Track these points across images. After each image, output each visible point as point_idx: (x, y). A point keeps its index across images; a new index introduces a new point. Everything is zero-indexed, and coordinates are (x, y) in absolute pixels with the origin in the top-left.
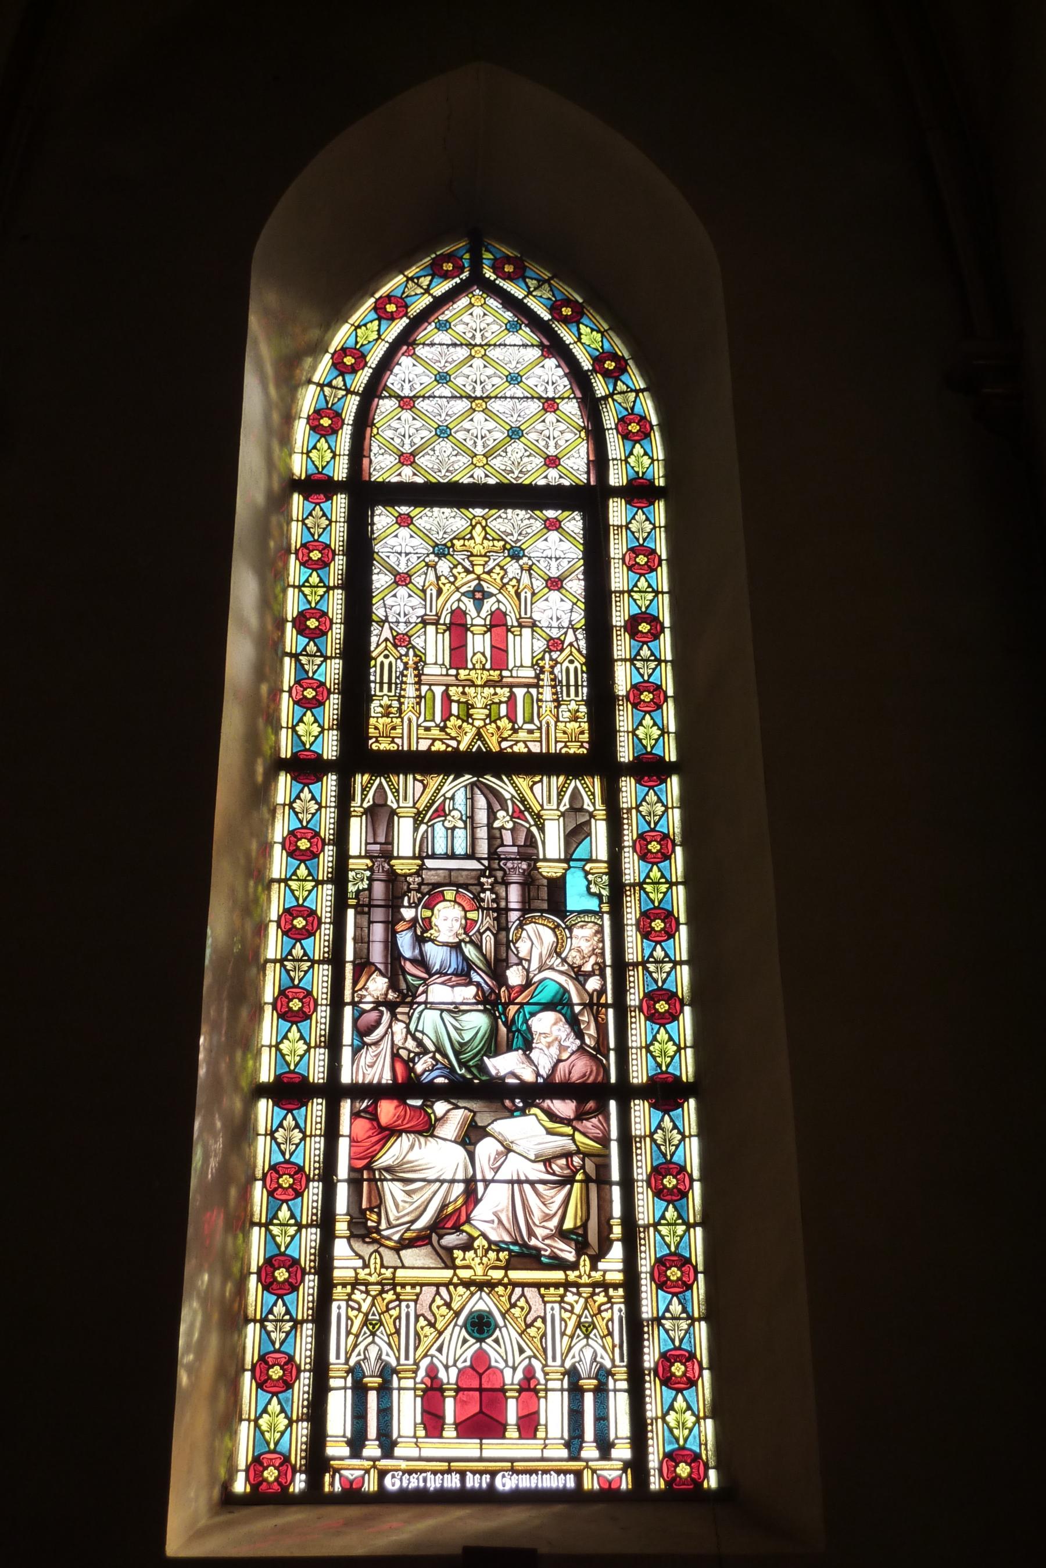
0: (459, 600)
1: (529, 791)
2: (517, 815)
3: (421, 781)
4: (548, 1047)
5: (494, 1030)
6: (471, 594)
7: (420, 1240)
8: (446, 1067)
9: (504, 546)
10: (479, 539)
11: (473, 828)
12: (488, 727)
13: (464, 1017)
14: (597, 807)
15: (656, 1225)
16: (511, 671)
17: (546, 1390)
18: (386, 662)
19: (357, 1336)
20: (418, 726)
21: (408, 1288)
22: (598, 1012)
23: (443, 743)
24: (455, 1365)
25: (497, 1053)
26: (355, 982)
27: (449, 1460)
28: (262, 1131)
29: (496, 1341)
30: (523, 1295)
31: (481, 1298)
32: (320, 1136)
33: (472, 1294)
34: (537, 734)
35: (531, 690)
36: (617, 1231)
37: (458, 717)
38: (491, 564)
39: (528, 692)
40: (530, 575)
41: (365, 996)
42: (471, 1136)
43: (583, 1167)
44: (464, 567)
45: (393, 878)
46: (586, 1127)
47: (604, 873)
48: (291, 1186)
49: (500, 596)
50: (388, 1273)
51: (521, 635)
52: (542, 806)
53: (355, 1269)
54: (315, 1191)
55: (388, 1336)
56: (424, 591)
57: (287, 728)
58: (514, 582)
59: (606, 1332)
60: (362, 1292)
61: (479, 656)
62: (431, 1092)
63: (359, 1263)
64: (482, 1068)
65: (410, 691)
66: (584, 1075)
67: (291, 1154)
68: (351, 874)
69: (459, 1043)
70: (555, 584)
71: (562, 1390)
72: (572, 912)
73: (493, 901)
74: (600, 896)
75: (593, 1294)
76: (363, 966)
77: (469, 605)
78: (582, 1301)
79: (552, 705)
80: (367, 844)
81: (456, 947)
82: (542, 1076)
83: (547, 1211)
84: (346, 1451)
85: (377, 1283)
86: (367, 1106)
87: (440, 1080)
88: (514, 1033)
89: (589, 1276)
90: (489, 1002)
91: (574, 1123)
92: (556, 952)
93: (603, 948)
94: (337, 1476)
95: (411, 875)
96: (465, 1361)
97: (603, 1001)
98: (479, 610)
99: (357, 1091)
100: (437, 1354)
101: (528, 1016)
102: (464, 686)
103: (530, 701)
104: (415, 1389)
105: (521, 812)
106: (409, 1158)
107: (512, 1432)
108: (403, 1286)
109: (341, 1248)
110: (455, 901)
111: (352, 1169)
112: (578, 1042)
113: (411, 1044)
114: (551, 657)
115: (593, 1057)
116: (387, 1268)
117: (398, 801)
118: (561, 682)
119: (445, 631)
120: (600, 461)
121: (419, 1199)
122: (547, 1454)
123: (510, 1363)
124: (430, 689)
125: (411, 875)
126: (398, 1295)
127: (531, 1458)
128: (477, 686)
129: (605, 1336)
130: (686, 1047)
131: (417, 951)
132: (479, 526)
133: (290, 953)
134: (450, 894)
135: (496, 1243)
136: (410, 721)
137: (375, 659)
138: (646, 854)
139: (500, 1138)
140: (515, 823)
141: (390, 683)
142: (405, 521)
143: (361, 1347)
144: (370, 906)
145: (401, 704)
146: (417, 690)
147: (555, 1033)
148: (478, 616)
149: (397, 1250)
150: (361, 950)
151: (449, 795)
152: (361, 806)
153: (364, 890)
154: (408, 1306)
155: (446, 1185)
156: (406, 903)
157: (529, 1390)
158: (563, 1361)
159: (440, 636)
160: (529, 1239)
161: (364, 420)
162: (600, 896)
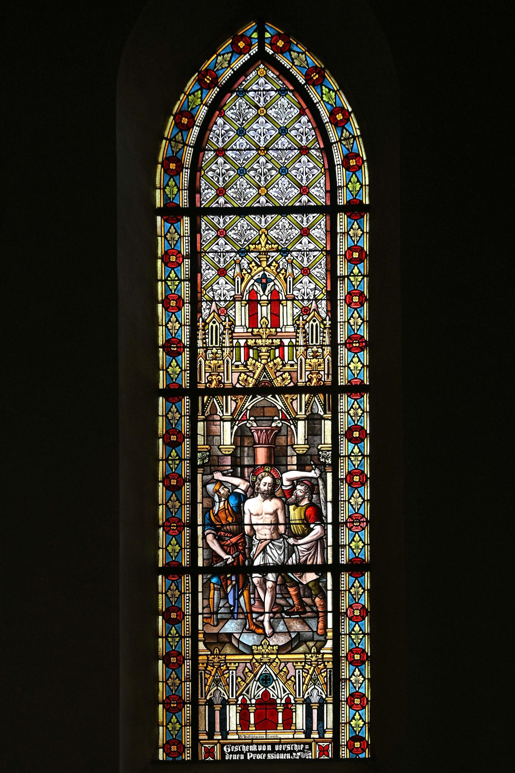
0: (253, 285)
9: (278, 247)
10: (263, 244)
12: (269, 364)
18: (214, 326)
20: (232, 364)
21: (233, 665)
23: (245, 374)
24: (254, 698)
29: (273, 687)
30: (285, 666)
31: (266, 668)
33: (262, 666)
35: (292, 340)
36: (330, 634)
37: (253, 358)
38: (271, 260)
39: (291, 341)
40: (292, 266)
44: (255, 263)
47: (328, 451)
49: (276, 281)
50: (223, 657)
56: (234, 280)
57: (163, 416)
60: (211, 666)
61: (264, 319)
63: (209, 653)
68: (199, 455)
70: (306, 271)
75: (318, 665)
77: (258, 288)
78: (312, 668)
79: (303, 349)
84: (206, 737)
96: (259, 696)
98: (264, 290)
102: (256, 339)
107: (280, 728)
108: (230, 663)
109: (201, 646)
114: (303, 318)
117: (222, 411)
118: (309, 334)
122: (296, 736)
124: (238, 342)
127: (288, 738)
132: (263, 234)
136: (228, 361)
137: (208, 324)
140: (282, 423)
142: (222, 233)
145: (223, 351)
148: (264, 294)
154: (232, 673)
158: (303, 696)
159: (243, 308)
161: (196, 167)
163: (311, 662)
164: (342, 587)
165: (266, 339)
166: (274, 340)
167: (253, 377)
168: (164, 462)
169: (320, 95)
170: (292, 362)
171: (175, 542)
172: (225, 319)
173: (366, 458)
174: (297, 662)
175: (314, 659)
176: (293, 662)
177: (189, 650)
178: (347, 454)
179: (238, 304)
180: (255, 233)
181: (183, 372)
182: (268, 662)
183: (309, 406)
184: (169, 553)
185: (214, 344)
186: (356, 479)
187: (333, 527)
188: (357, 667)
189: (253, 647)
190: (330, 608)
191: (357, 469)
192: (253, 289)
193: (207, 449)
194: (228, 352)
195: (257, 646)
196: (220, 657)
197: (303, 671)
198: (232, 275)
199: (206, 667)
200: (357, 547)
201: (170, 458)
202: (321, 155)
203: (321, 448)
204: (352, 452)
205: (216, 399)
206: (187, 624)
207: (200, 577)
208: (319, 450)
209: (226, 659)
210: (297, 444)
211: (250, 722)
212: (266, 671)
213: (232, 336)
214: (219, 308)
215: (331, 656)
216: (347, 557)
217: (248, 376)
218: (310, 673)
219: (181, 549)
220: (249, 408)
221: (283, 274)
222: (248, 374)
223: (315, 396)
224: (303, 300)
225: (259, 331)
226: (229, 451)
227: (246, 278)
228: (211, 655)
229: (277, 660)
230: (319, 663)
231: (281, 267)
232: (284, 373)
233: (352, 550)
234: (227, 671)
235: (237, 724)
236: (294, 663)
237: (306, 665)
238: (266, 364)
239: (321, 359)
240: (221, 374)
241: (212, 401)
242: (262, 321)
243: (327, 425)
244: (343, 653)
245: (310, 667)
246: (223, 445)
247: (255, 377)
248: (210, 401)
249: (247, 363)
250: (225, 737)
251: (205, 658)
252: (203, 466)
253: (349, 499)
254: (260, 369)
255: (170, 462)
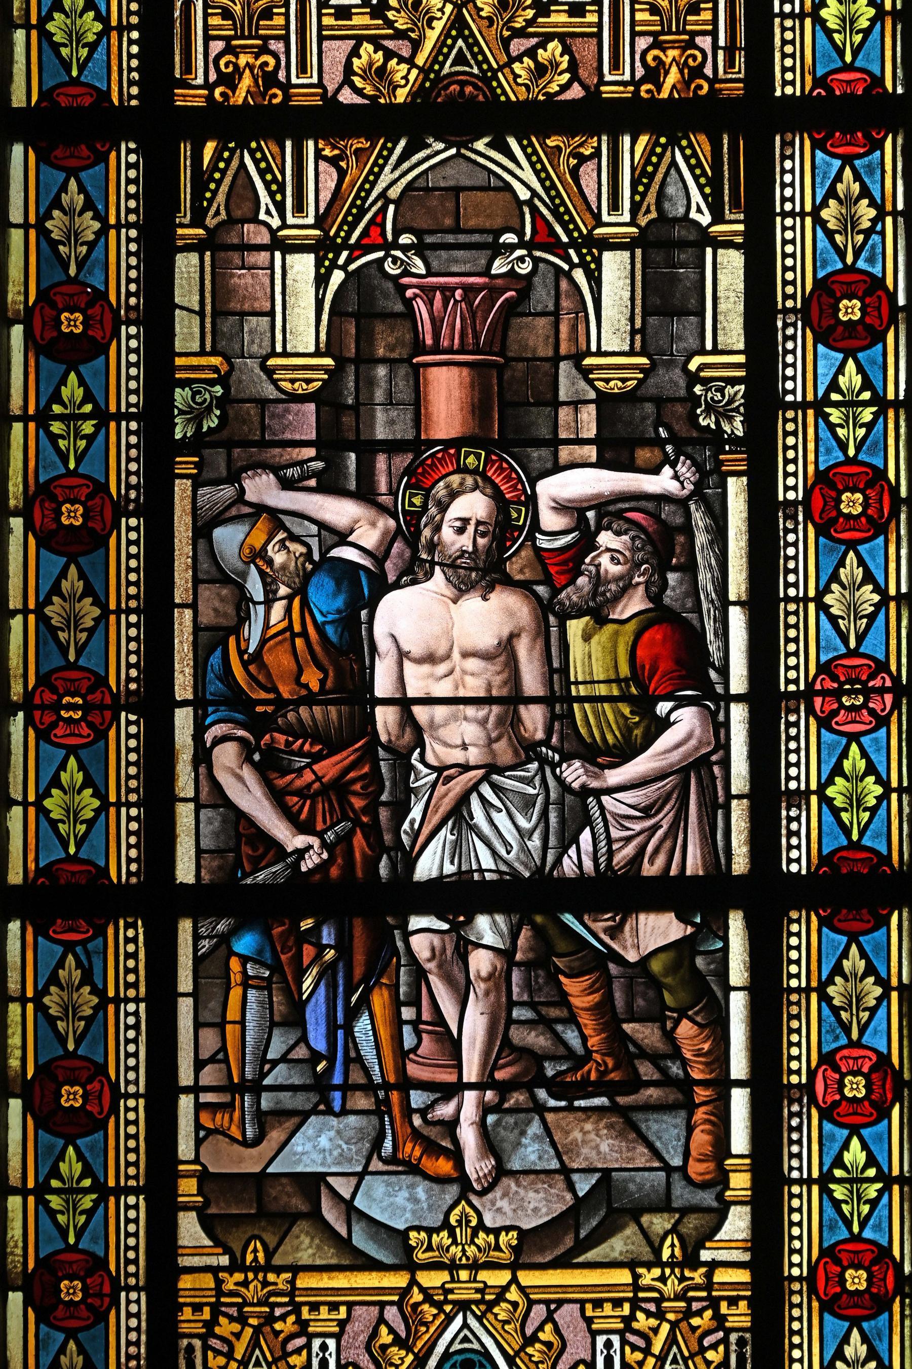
21: (324, 1312)
30: (550, 1318)
33: (449, 1319)
34: (592, 18)
36: (740, 1182)
52: (597, 217)
53: (214, 1270)
60: (232, 1319)
63: (225, 1260)
68: (181, 396)
75: (688, 1314)
78: (666, 1327)
108: (314, 1307)
109: (189, 1229)
116: (278, 1270)
117: (280, 208)
140: (536, 261)
163: (658, 1301)
164: (790, 976)
167: (410, 61)
168: (32, 426)
171: (79, 777)
173: (891, 414)
174: (598, 1304)
175: (671, 1287)
176: (582, 1303)
177: (136, 1248)
178: (810, 397)
181: (114, 35)
182: (477, 1303)
183: (647, 187)
184: (54, 824)
186: (852, 503)
187: (751, 712)
188: (855, 1322)
189: (413, 1234)
190: (739, 1067)
191: (854, 461)
193: (215, 369)
195: (430, 1231)
196: (271, 1277)
197: (624, 1342)
199: (210, 1325)
200: (856, 801)
201: (57, 409)
203: (702, 367)
204: (834, 386)
205: (252, 153)
206: (128, 1137)
207: (185, 927)
208: (693, 378)
209: (294, 1288)
210: (600, 353)
212: (466, 1339)
215: (743, 1276)
216: (814, 846)
217: (389, 55)
218: (657, 1349)
219: (105, 805)
220: (394, 193)
222: (389, 44)
223: (673, 142)
226: (308, 381)
229: (513, 1295)
230: (696, 1306)
232: (543, 45)
233: (836, 812)
234: (300, 1341)
236: (589, 1306)
237: (640, 1315)
240: (277, 46)
241: (235, 164)
243: (729, 270)
244: (796, 1265)
245: (653, 1322)
246: (285, 354)
247: (420, 60)
248: (228, 162)
251: (208, 1281)
252: (197, 443)
253: (822, 592)
255: (56, 427)
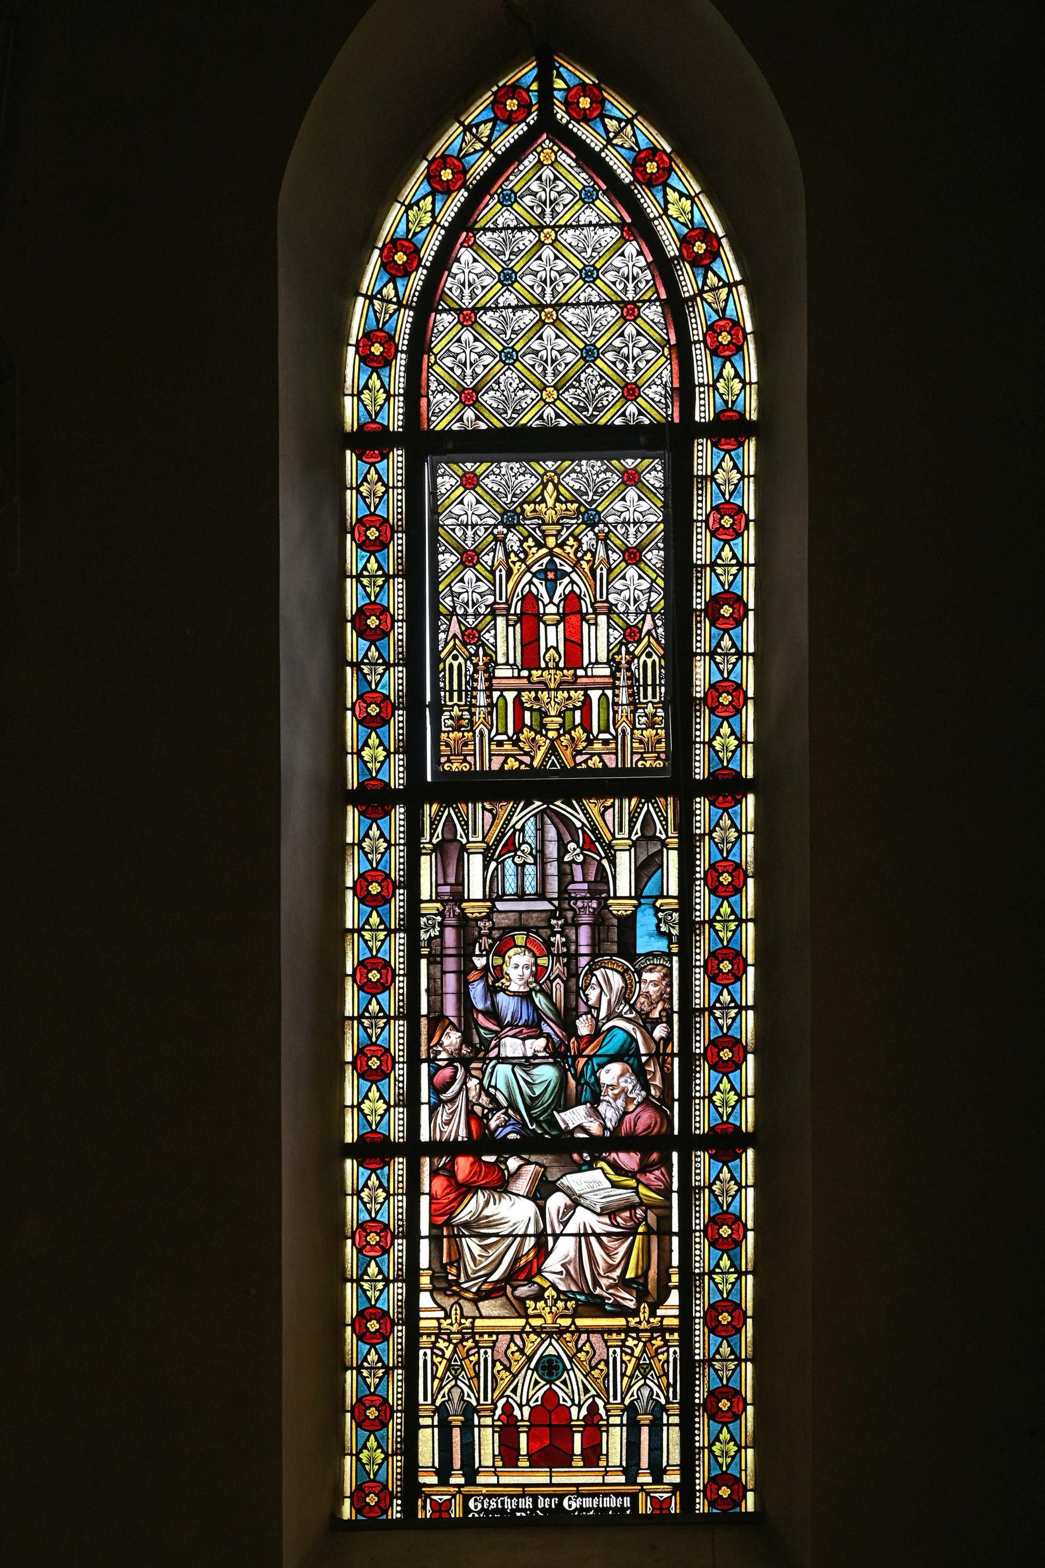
0: (530, 582)
1: (599, 819)
2: (588, 845)
3: (490, 811)
4: (615, 1099)
5: (563, 1082)
6: (542, 574)
7: (495, 1292)
8: (518, 1123)
9: (578, 508)
10: (550, 502)
11: (544, 864)
12: (562, 738)
13: (536, 1071)
14: (670, 835)
15: (711, 1273)
16: (585, 669)
17: (608, 1425)
18: (455, 664)
19: (442, 1380)
20: (491, 740)
21: (486, 1337)
22: (664, 1061)
24: (528, 1404)
25: (565, 1109)
26: (430, 1038)
27: (523, 1486)
28: (349, 1191)
29: (564, 1382)
30: (588, 1340)
31: (550, 1344)
32: (402, 1194)
33: (543, 1341)
36: (675, 1279)
37: (531, 728)
38: (565, 533)
39: (604, 694)
40: (606, 546)
41: (440, 1052)
42: (540, 1193)
43: (645, 1219)
44: (535, 540)
45: (464, 923)
46: (649, 1179)
47: (674, 910)
48: (378, 1243)
49: (574, 576)
50: (468, 1323)
51: (596, 624)
52: (613, 835)
53: (438, 1319)
54: (400, 1245)
55: (469, 1379)
56: (492, 572)
58: (588, 557)
59: (662, 1373)
60: (445, 1340)
61: (552, 651)
62: (505, 1148)
63: (441, 1314)
64: (553, 1123)
65: (482, 699)
66: (649, 1127)
67: (377, 1213)
69: (530, 1097)
70: (633, 556)
71: (621, 1425)
72: (640, 955)
73: (563, 944)
74: (669, 936)
75: (652, 1338)
76: (438, 1021)
78: (641, 1344)
79: (628, 709)
80: (437, 885)
81: (526, 997)
82: (609, 1129)
83: (611, 1262)
84: (434, 1480)
85: (458, 1332)
86: (445, 1164)
87: (512, 1136)
88: (583, 1085)
89: (648, 1322)
90: (557, 1055)
91: (638, 1176)
92: (624, 998)
93: (671, 993)
94: (428, 1501)
95: (481, 919)
96: (537, 1400)
97: (669, 1051)
99: (435, 1148)
100: (512, 1395)
101: (596, 1068)
102: (536, 691)
103: (605, 706)
104: (493, 1426)
105: (593, 843)
106: (486, 1212)
107: (578, 1462)
108: (481, 1334)
109: (425, 1300)
110: (525, 947)
111: (432, 1225)
112: (644, 1093)
113: (484, 1100)
114: (627, 649)
115: (658, 1109)
116: (467, 1318)
118: (638, 680)
119: (516, 622)
120: (684, 391)
121: (494, 1253)
122: (609, 1479)
123: (576, 1402)
124: (502, 695)
125: (481, 919)
126: (476, 1342)
128: (551, 690)
129: (660, 1377)
130: (747, 1096)
131: (489, 1003)
132: (550, 484)
133: (366, 1009)
134: (520, 939)
135: (564, 1293)
136: (481, 734)
138: (717, 887)
139: (569, 1192)
140: (585, 855)
141: (460, 691)
142: (470, 482)
143: (446, 1390)
144: (443, 956)
145: (472, 714)
146: (488, 697)
147: (623, 1085)
148: (551, 602)
149: (475, 1302)
150: (434, 1003)
151: (518, 826)
152: (430, 842)
153: (436, 937)
154: (486, 1353)
155: (518, 1239)
156: (477, 952)
157: (593, 1425)
158: (623, 1399)
159: (511, 629)
160: (595, 1289)
162: (669, 936)
165: (557, 690)
166: (572, 693)
169: (662, 204)
170: (607, 736)
172: (477, 651)
179: (501, 622)
180: (534, 480)
185: (455, 700)
192: (530, 591)
194: (482, 716)
197: (622, 1351)
198: (490, 563)
202: (662, 321)
203: (661, 905)
211: (519, 1449)
213: (491, 685)
214: (463, 628)
221: (588, 562)
224: (627, 612)
225: (541, 676)
227: (515, 571)
228: (445, 1318)
231: (585, 548)
235: (494, 1456)
238: (555, 740)
239: (662, 729)
242: (548, 655)
249: (518, 737)
250: (471, 1481)
254: (543, 749)
